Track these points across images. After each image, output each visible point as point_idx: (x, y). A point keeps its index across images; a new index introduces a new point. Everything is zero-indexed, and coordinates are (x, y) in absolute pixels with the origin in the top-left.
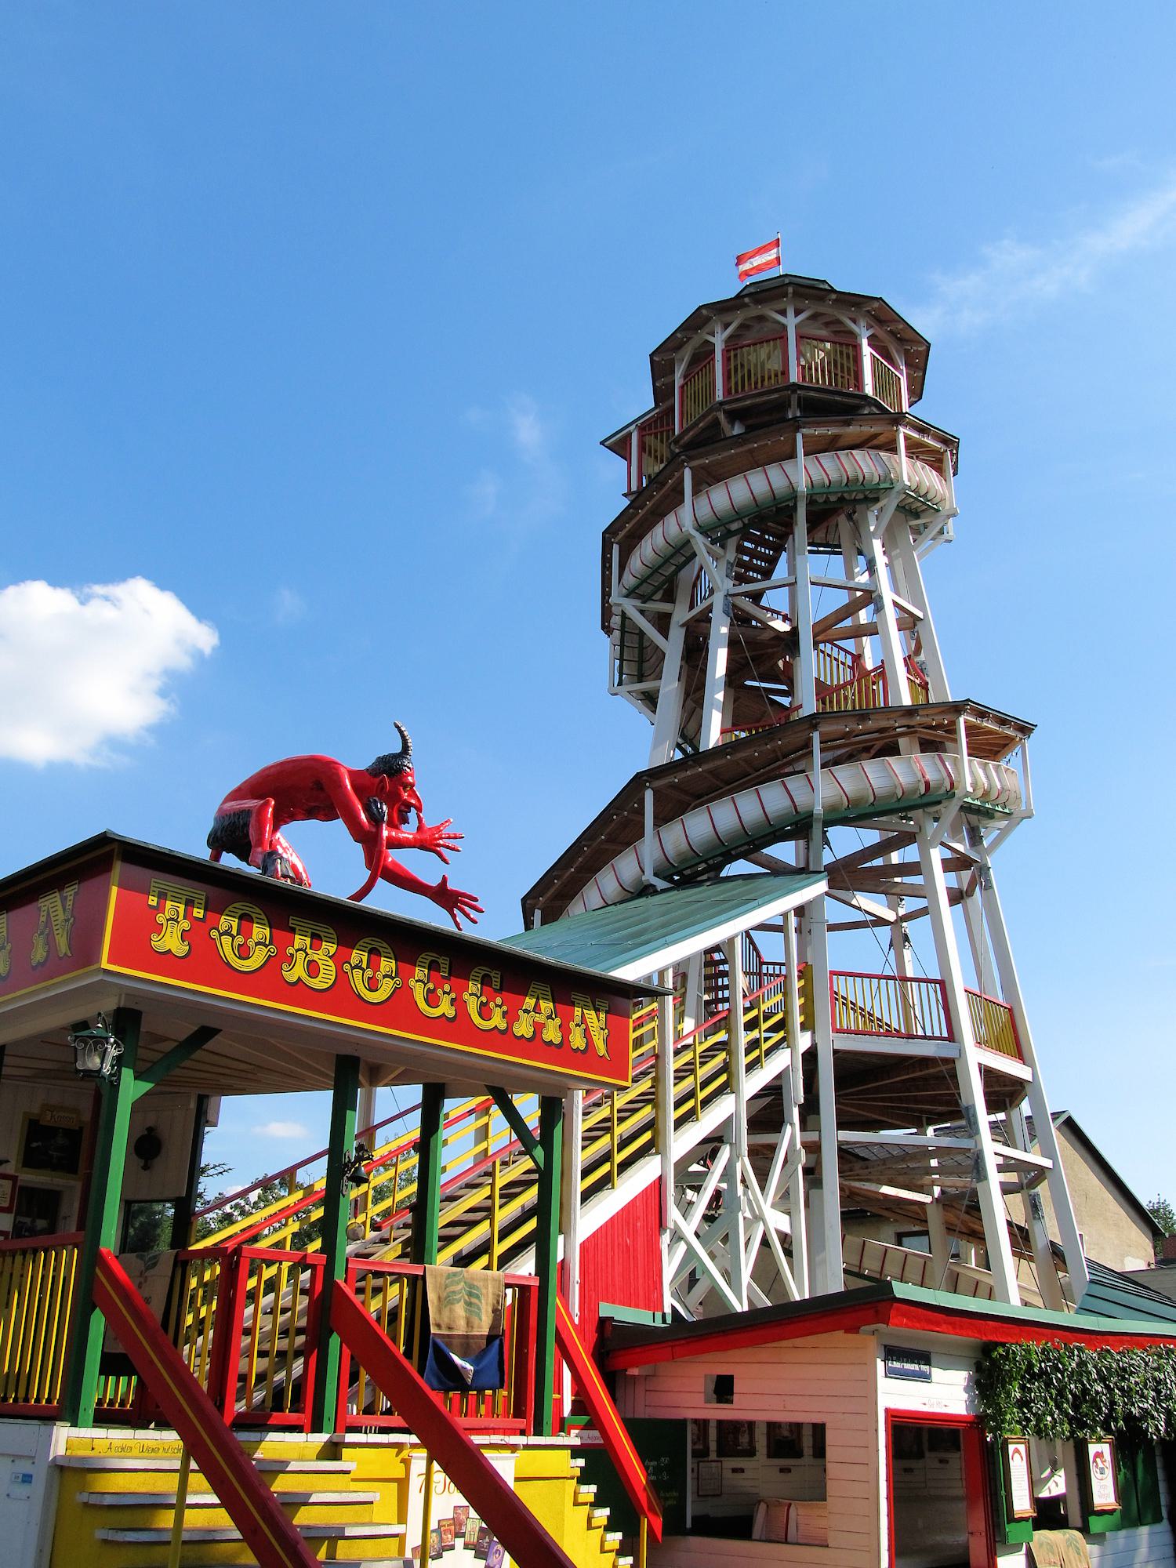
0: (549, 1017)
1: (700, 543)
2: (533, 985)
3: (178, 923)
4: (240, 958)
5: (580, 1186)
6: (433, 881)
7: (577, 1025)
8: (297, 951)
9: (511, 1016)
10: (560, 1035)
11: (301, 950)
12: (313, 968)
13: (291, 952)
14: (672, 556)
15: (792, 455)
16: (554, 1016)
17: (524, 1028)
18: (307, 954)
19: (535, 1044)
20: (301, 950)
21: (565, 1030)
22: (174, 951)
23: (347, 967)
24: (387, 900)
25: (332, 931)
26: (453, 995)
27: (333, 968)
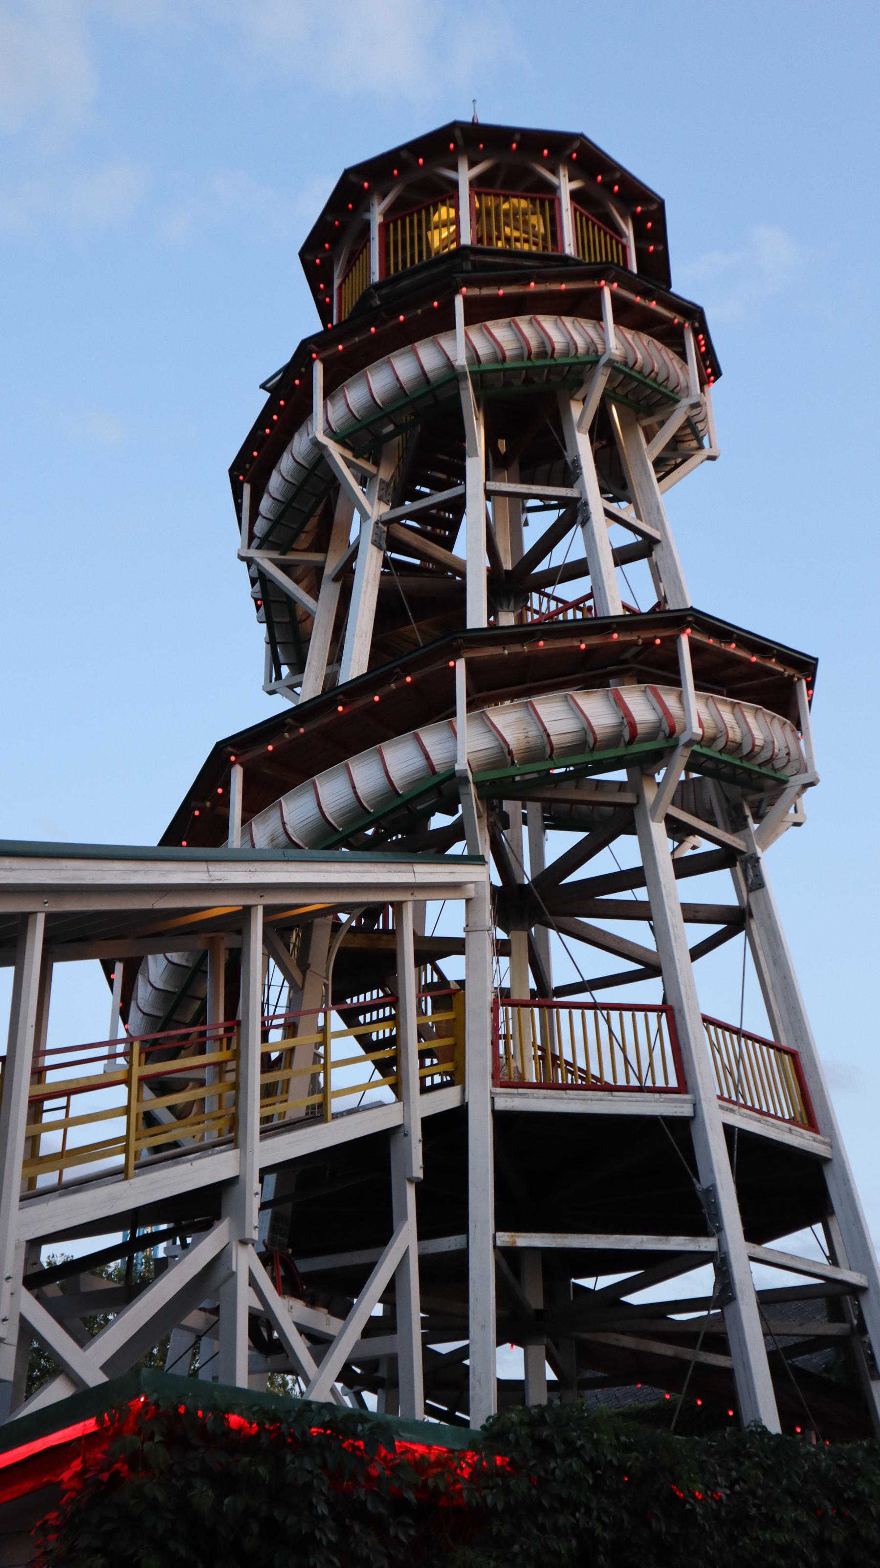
15: (451, 326)
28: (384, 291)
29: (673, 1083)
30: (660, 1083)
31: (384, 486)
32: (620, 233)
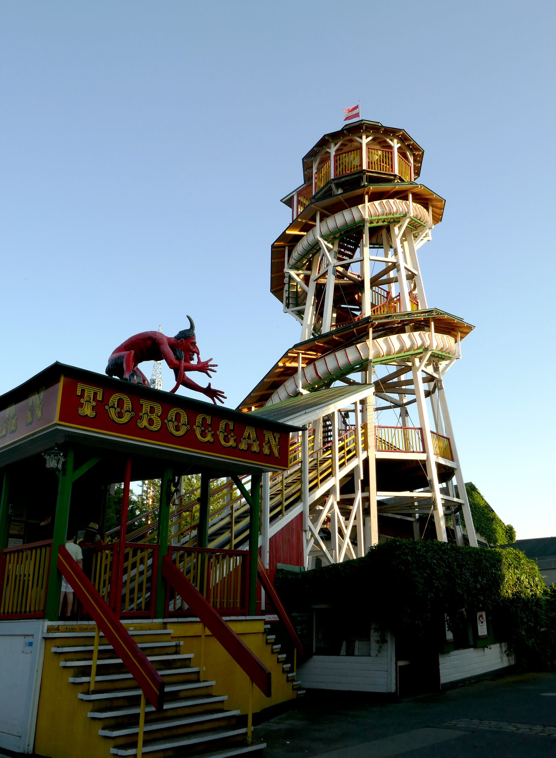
0: (254, 441)
1: (324, 243)
2: (247, 427)
3: (90, 402)
4: (119, 417)
5: (269, 515)
6: (205, 386)
7: (266, 444)
8: (144, 414)
9: (238, 441)
10: (259, 448)
11: (146, 414)
12: (151, 422)
13: (141, 414)
14: (311, 250)
16: (256, 440)
17: (243, 446)
18: (148, 415)
19: (248, 454)
20: (146, 414)
21: (261, 446)
22: (89, 415)
23: (166, 421)
24: (183, 392)
25: (159, 405)
26: (213, 432)
27: (160, 422)
28: (336, 181)
29: (422, 450)
30: (418, 450)
31: (335, 253)
32: (409, 161)
